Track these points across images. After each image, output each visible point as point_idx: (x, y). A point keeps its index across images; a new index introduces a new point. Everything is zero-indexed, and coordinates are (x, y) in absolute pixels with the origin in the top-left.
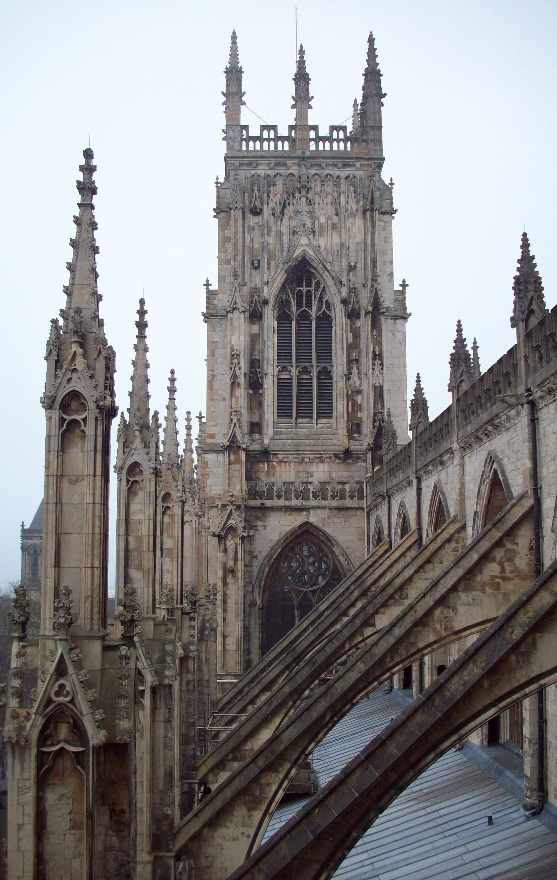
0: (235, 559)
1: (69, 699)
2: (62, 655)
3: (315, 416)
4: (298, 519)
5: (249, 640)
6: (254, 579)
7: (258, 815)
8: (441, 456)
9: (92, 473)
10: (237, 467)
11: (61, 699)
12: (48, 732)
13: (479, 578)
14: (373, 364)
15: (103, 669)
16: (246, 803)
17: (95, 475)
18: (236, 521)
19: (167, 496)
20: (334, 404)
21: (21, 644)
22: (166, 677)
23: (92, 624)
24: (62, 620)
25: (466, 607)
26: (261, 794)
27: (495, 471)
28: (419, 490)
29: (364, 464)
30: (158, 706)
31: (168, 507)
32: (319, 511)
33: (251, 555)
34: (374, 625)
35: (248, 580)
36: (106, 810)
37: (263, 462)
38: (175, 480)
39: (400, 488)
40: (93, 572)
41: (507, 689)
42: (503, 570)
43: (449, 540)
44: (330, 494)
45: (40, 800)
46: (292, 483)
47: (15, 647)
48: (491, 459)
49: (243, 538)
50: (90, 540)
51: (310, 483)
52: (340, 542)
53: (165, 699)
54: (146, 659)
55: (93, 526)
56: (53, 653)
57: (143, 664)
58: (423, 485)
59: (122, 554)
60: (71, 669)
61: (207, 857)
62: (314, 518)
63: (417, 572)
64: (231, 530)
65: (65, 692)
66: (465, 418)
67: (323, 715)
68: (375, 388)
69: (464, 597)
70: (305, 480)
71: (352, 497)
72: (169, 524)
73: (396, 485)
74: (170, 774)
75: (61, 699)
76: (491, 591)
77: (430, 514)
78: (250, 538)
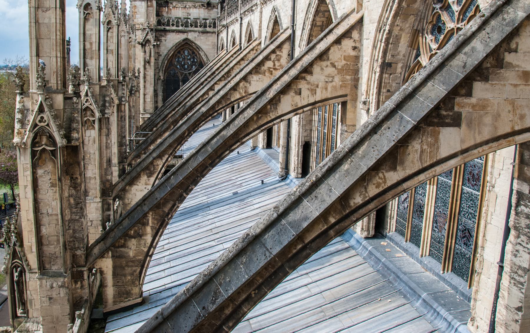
0: (150, 56)
1: (46, 124)
2: (41, 102)
4: (182, 37)
5: (157, 97)
6: (160, 67)
8: (252, 7)
9: (54, 6)
10: (150, 9)
11: (42, 124)
12: (36, 140)
13: (263, 68)
15: (64, 109)
16: (147, 174)
17: (56, 8)
18: (150, 37)
19: (109, 23)
21: (21, 96)
22: (106, 113)
23: (57, 86)
24: (40, 84)
25: (255, 82)
26: (153, 170)
27: (276, 17)
28: (241, 24)
29: (216, 10)
30: (102, 128)
31: (110, 28)
32: (193, 33)
33: (158, 54)
35: (156, 67)
36: (68, 177)
37: (165, 7)
38: (114, 14)
39: (232, 23)
40: (57, 59)
41: (265, 121)
42: (274, 65)
43: (252, 50)
44: (199, 24)
45: (34, 173)
46: (180, 18)
47: (18, 98)
48: (274, 10)
49: (154, 45)
50: (55, 43)
51: (189, 18)
52: (203, 49)
53: (106, 124)
54: (95, 104)
55: (56, 35)
56: (37, 101)
57: (94, 107)
58: (243, 22)
59: (82, 52)
60: (46, 109)
61: (128, 199)
62: (191, 36)
63: (236, 64)
64: (148, 41)
65: (44, 120)
67: (184, 133)
69: (254, 78)
70: (186, 17)
71: (210, 27)
73: (231, 22)
74: (109, 161)
75: (42, 124)
76: (268, 74)
77: (246, 37)
78: (158, 46)
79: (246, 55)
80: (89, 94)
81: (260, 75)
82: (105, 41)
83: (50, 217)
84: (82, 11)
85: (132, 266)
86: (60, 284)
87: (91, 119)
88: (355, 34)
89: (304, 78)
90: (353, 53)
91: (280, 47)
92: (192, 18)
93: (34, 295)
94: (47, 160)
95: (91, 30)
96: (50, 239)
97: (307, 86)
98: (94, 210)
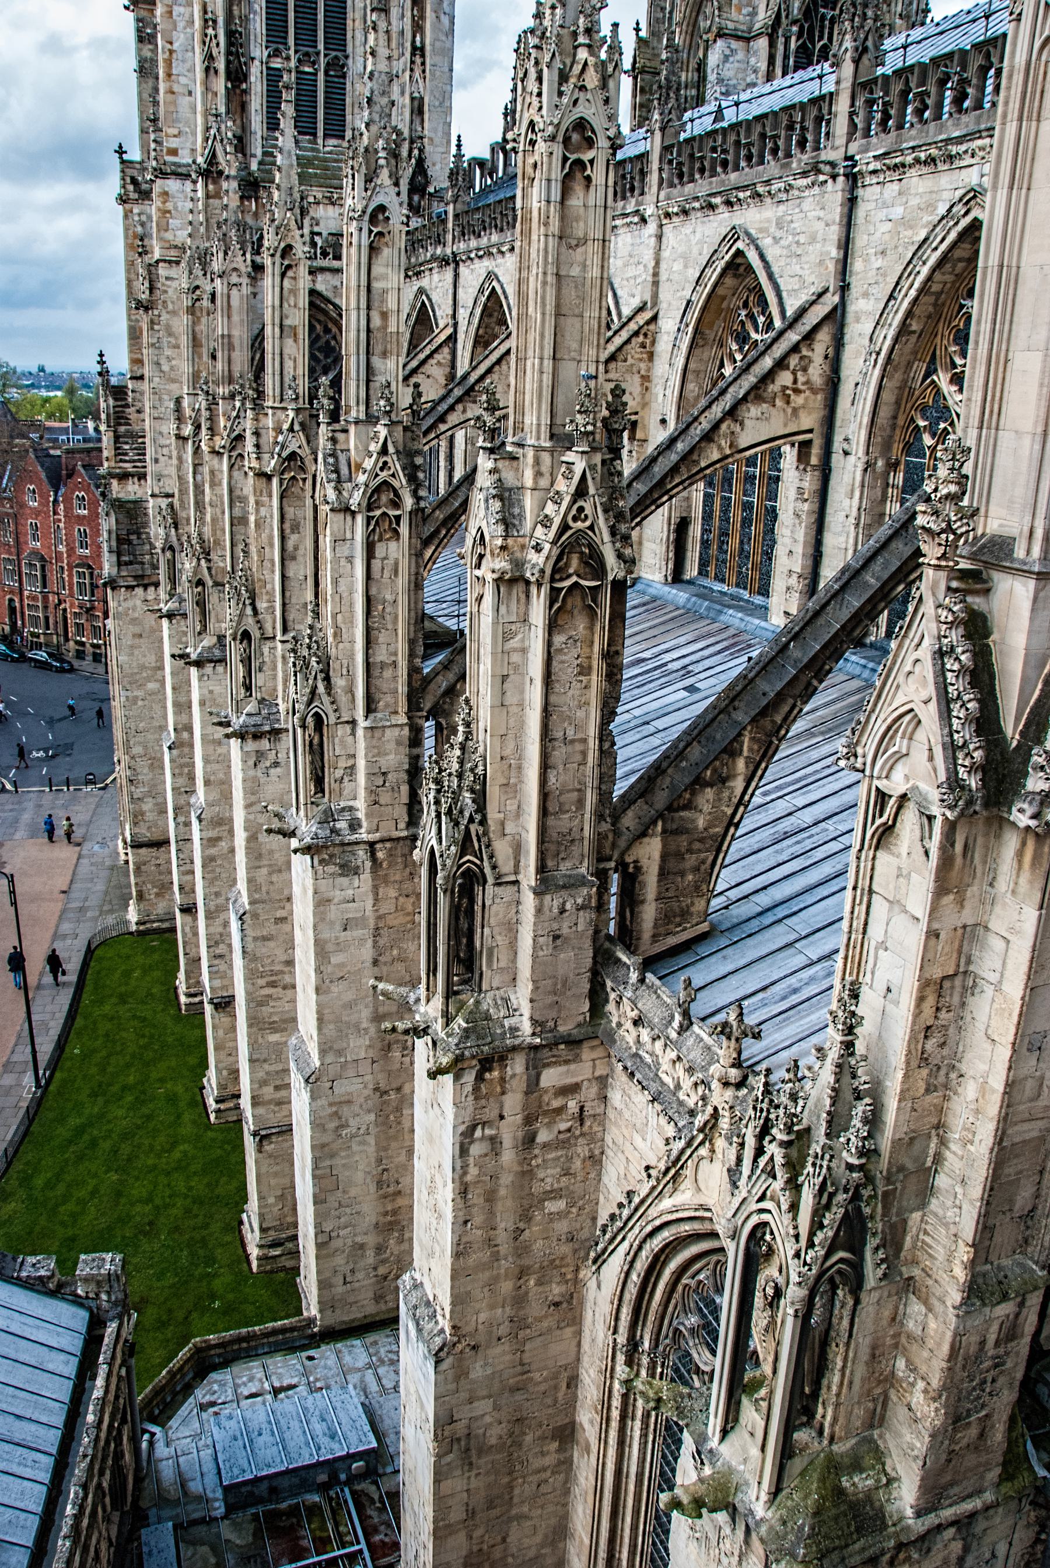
1: (588, 523)
3: (320, 133)
14: (412, 62)
19: (288, 250)
20: (349, 118)
31: (289, 267)
32: (328, 276)
42: (795, 381)
43: (636, 334)
51: (319, 234)
59: (363, 335)
60: (592, 491)
66: (681, 176)
68: (413, 99)
69: (753, 411)
72: (291, 291)
75: (579, 525)
79: (620, 349)
80: (391, 449)
82: (277, 303)
83: (570, 748)
84: (365, 226)
85: (700, 851)
86: (580, 901)
87: (393, 513)
91: (809, 337)
92: (325, 234)
93: (498, 938)
95: (385, 277)
96: (562, 799)
98: (392, 746)
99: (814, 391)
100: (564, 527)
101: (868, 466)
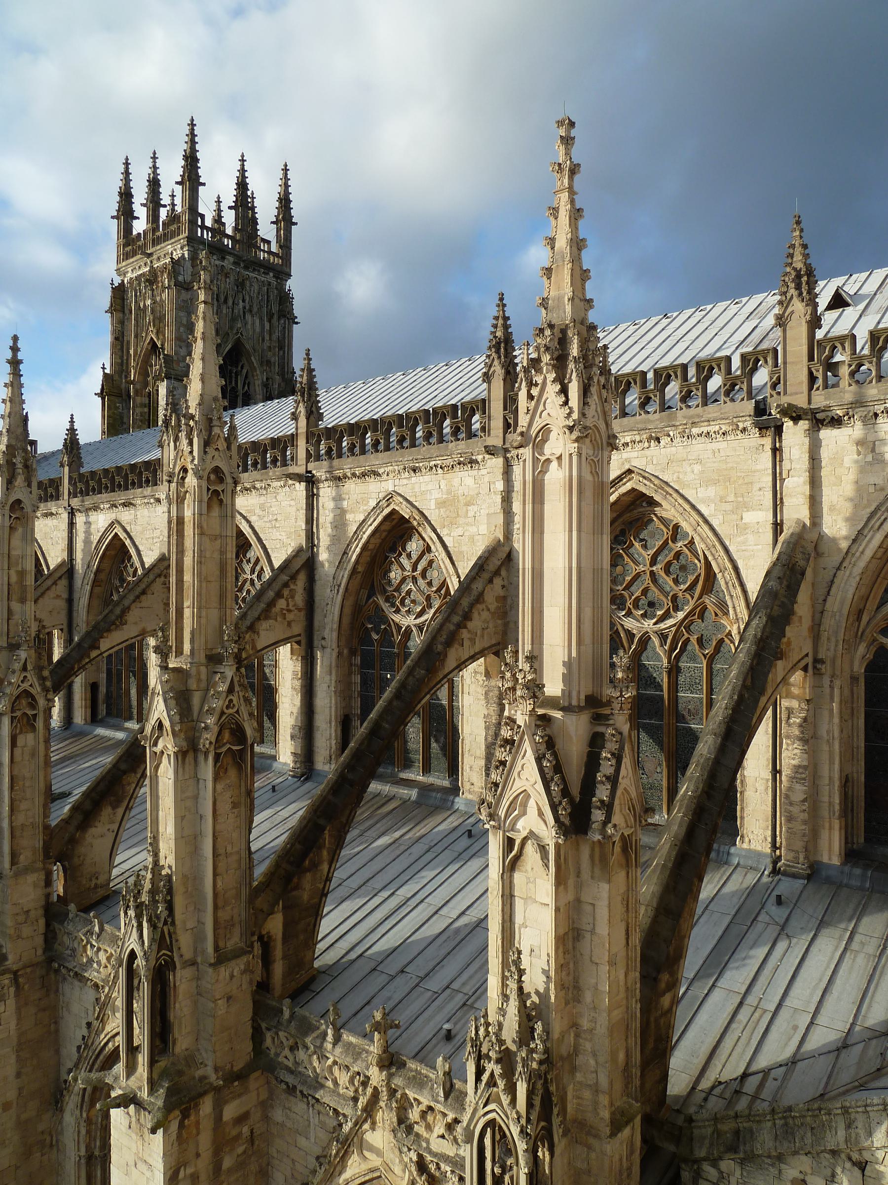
1: (235, 710)
7: (120, 811)
11: (231, 711)
13: (274, 610)
34: (98, 648)
42: (288, 605)
61: (79, 857)
69: (264, 625)
75: (231, 711)
79: (148, 586)
80: (29, 668)
81: (271, 621)
88: (503, 573)
89: (465, 627)
90: (501, 593)
94: (229, 767)
97: (469, 636)
99: (300, 610)
100: (222, 713)
101: (340, 654)
